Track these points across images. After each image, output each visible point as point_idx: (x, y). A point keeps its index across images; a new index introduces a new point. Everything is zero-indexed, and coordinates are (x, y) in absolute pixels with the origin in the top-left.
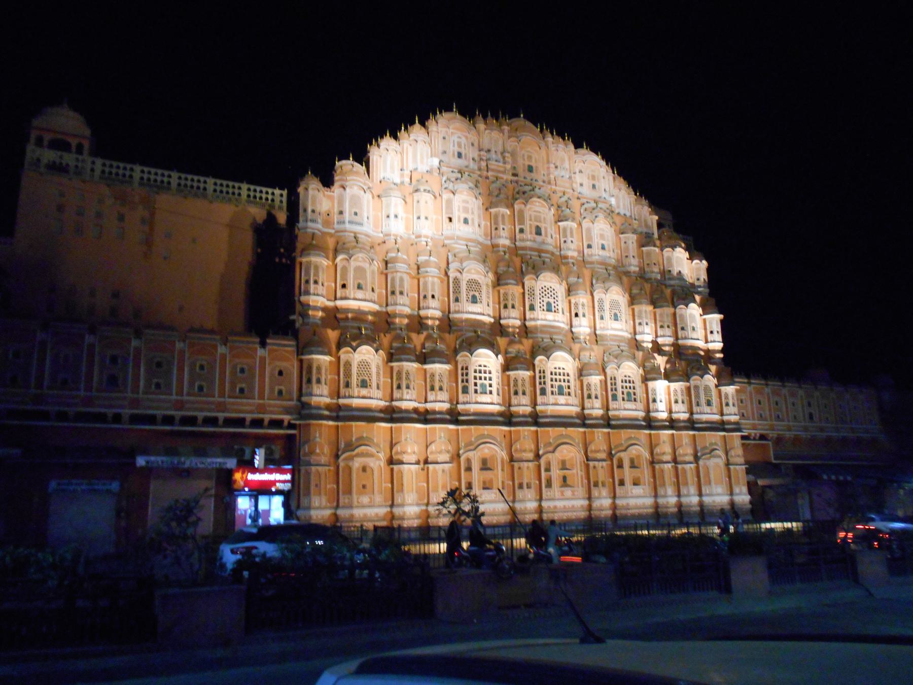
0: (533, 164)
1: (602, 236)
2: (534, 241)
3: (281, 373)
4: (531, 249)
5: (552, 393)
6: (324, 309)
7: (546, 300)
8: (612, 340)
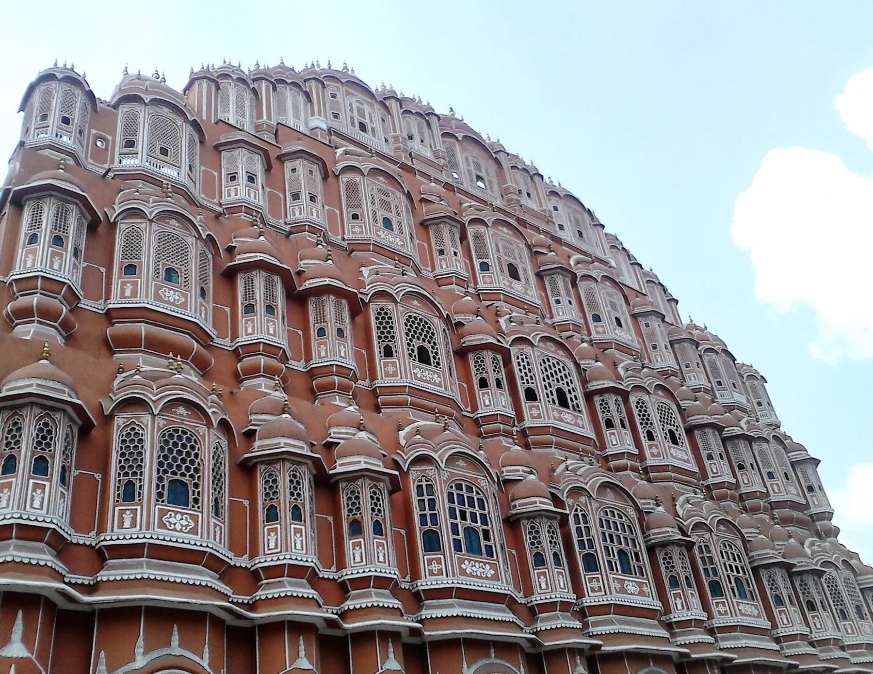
2: (510, 286)
7: (555, 386)
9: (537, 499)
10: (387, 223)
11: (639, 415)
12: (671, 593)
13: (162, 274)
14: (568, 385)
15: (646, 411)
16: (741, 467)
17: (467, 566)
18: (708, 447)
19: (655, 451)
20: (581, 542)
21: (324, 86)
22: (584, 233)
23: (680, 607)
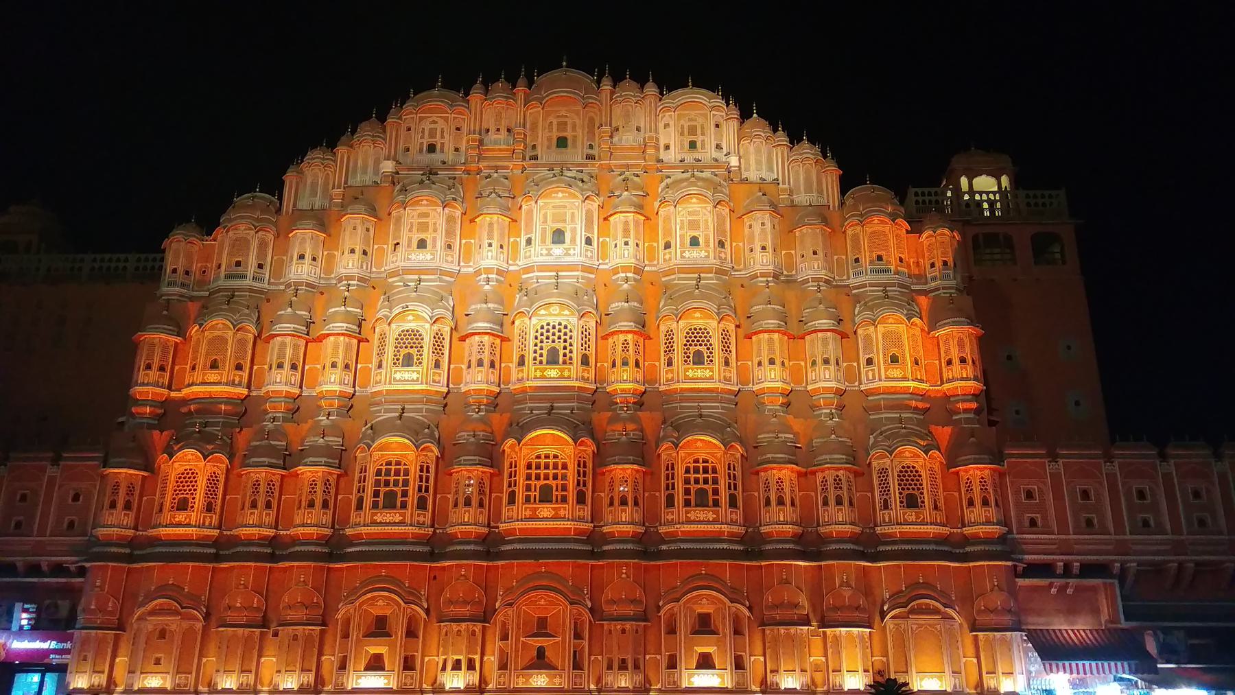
0: (568, 134)
1: (693, 225)
2: (549, 254)
3: (76, 498)
4: (542, 268)
5: (528, 500)
6: (154, 403)
7: (547, 345)
8: (532, 399)
10: (422, 244)
12: (607, 509)
13: (209, 363)
14: (565, 341)
16: (814, 363)
22: (699, 139)
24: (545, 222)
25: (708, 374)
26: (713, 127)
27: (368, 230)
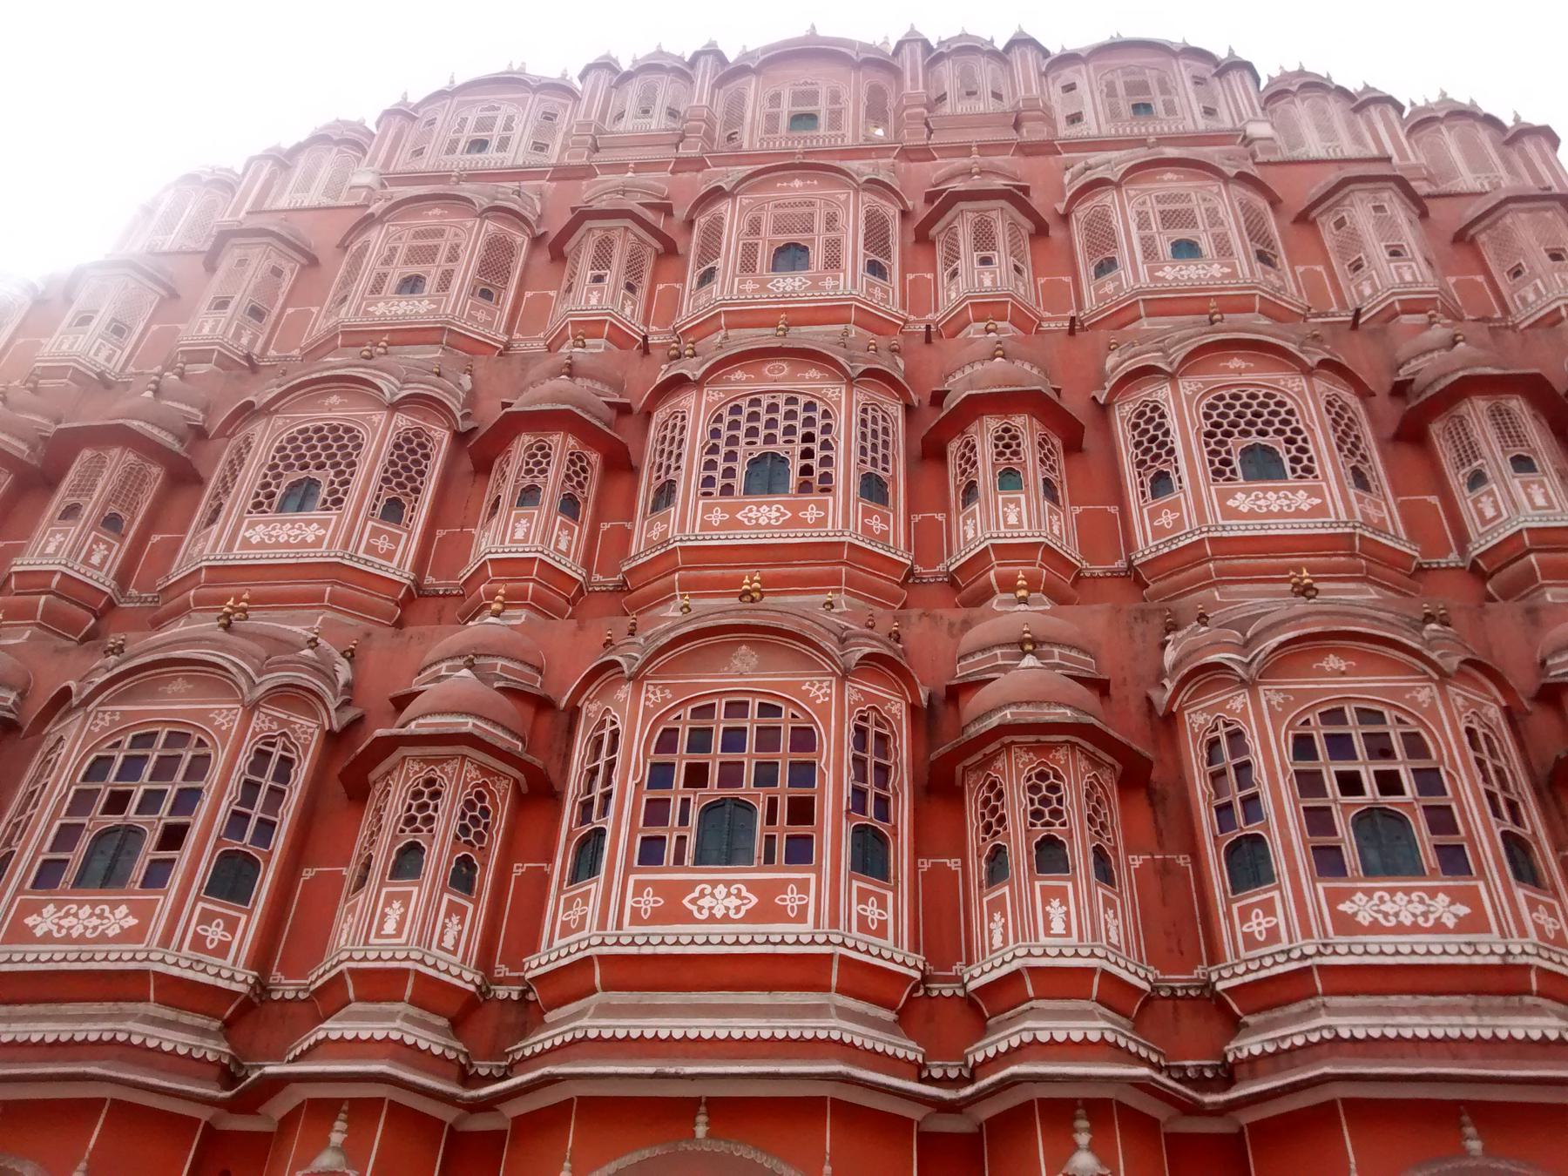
5: (651, 852)
9: (413, 724)
10: (412, 285)
11: (1138, 445)
12: (981, 901)
14: (808, 438)
15: (1161, 425)
17: (44, 922)
18: (1469, 452)
19: (1167, 519)
20: (587, 806)
21: (414, 119)
23: (997, 941)
24: (755, 227)
25: (1303, 501)
26: (1189, 84)
27: (277, 272)
